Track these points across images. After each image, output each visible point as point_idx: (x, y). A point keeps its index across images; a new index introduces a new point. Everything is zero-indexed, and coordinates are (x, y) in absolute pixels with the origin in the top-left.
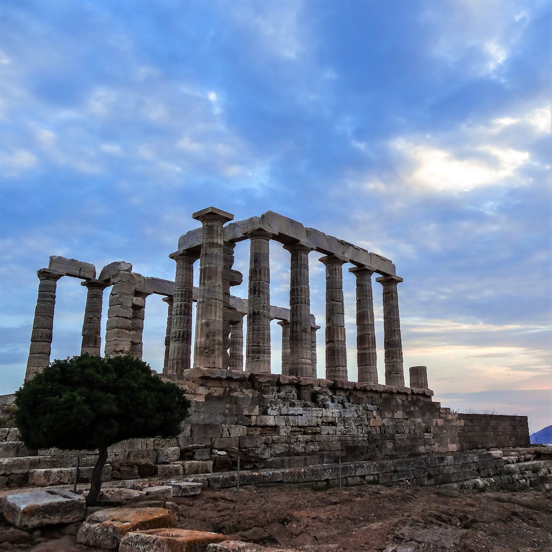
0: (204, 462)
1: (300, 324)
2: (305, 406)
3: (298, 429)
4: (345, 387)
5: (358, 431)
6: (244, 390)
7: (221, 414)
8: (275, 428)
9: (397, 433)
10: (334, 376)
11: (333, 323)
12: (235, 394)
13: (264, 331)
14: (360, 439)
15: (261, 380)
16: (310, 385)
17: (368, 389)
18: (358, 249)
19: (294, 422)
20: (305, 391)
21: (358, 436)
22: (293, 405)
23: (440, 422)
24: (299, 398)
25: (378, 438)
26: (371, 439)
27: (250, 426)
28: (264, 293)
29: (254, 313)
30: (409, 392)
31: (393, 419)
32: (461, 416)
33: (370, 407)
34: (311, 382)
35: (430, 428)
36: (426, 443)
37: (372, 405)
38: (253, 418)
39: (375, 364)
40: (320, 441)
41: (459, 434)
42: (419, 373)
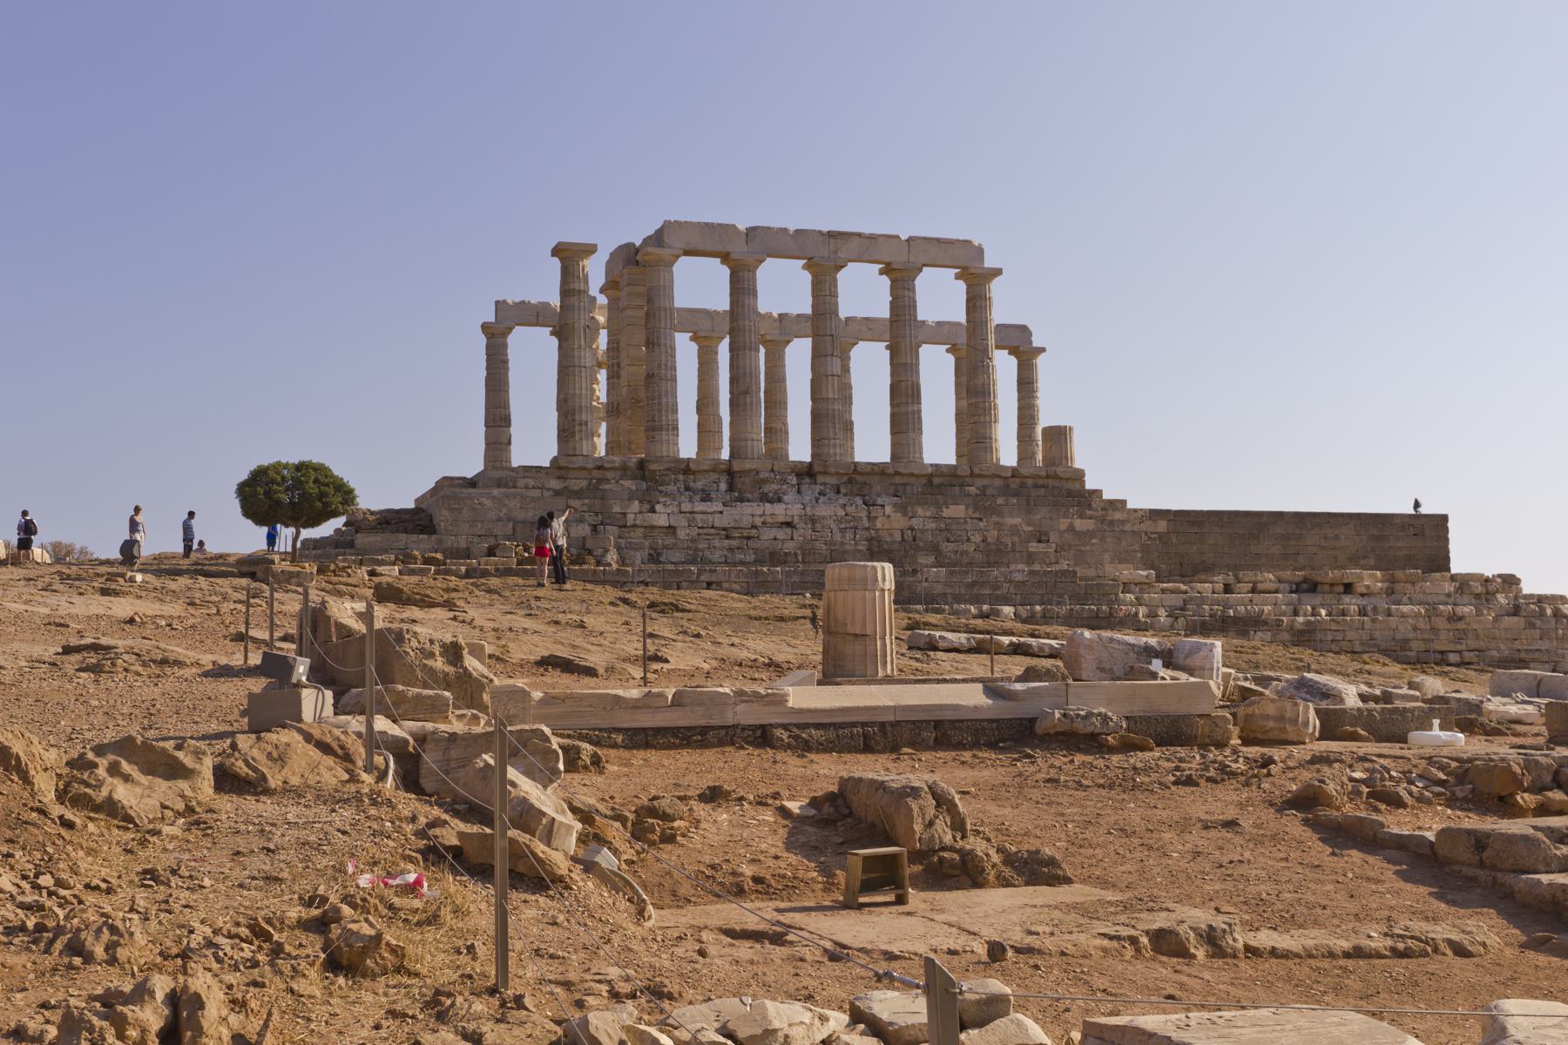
8: (671, 529)
15: (653, 467)
18: (872, 237)
22: (706, 498)
23: (1079, 524)
24: (731, 489)
31: (936, 518)
32: (1155, 514)
35: (1047, 534)
38: (630, 517)
42: (1059, 436)
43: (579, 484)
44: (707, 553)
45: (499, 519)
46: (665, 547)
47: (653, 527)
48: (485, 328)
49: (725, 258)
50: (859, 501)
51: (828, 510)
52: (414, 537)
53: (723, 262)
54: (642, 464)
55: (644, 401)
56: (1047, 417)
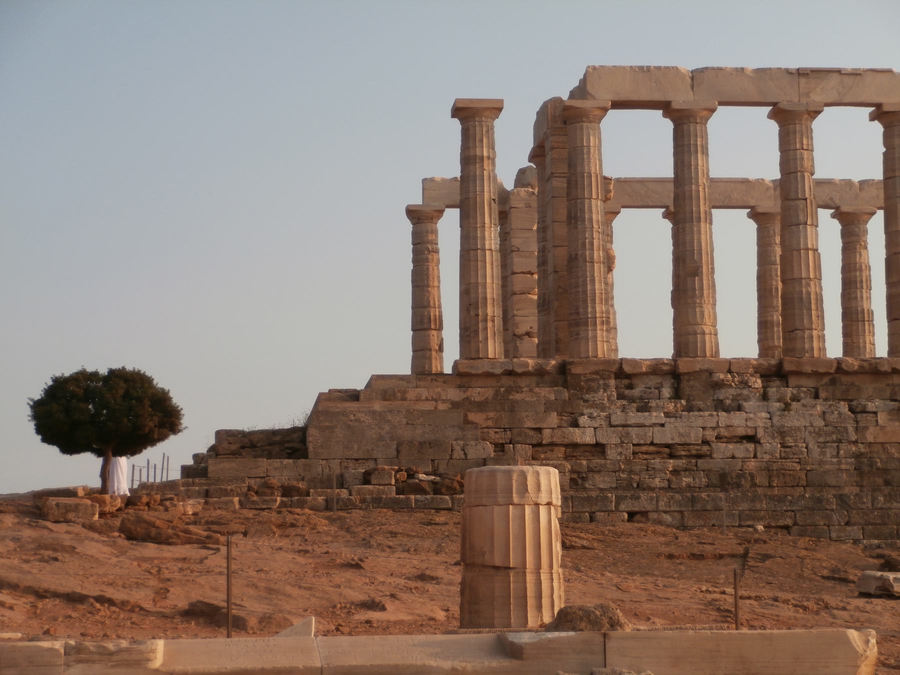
0: (381, 487)
3: (652, 449)
4: (808, 369)
5: (823, 453)
6: (537, 390)
7: (454, 426)
8: (599, 448)
12: (517, 396)
13: (585, 285)
16: (701, 371)
18: (856, 74)
20: (691, 383)
21: (821, 463)
22: (644, 408)
24: (677, 395)
27: (540, 445)
29: (571, 256)
34: (706, 367)
38: (547, 432)
40: (710, 470)
43: (478, 393)
44: (645, 476)
45: (381, 438)
46: (590, 470)
47: (575, 446)
48: (413, 213)
49: (666, 108)
50: (844, 407)
51: (806, 417)
52: (277, 463)
53: (665, 115)
54: (563, 369)
55: (568, 288)
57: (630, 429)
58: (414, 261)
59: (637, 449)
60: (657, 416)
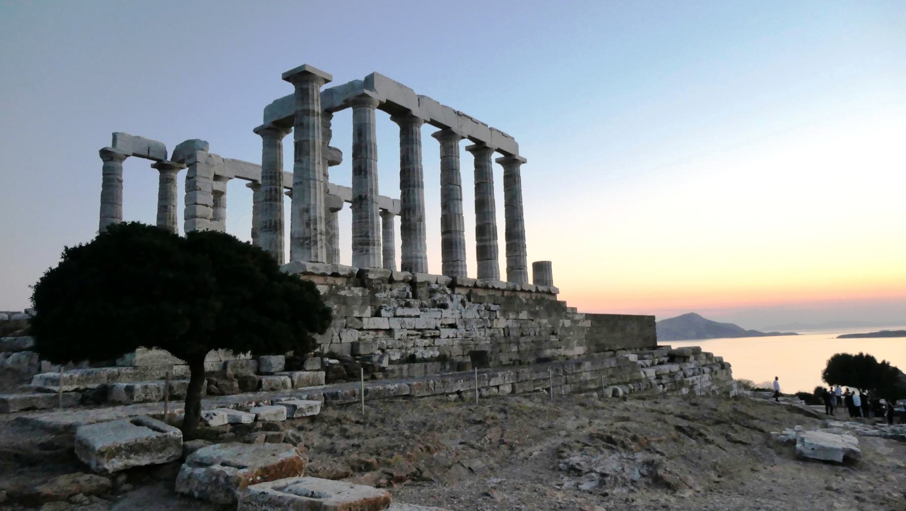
1: (414, 212)
2: (422, 307)
3: (415, 332)
4: (465, 284)
6: (353, 288)
8: (390, 332)
9: (522, 335)
10: (452, 272)
11: (449, 211)
12: (343, 293)
13: (372, 218)
14: (483, 342)
15: (371, 276)
17: (490, 286)
19: (410, 324)
21: (480, 340)
22: (408, 305)
23: (567, 323)
25: (502, 341)
26: (496, 343)
28: (371, 174)
30: (534, 290)
31: (516, 320)
32: (588, 316)
33: (493, 307)
36: (552, 346)
37: (494, 304)
38: (365, 320)
39: (495, 258)
41: (586, 336)
42: (542, 268)
48: (105, 154)
51: (472, 312)
56: (533, 254)
57: (405, 319)
58: (104, 185)
59: (410, 332)
60: (415, 311)
